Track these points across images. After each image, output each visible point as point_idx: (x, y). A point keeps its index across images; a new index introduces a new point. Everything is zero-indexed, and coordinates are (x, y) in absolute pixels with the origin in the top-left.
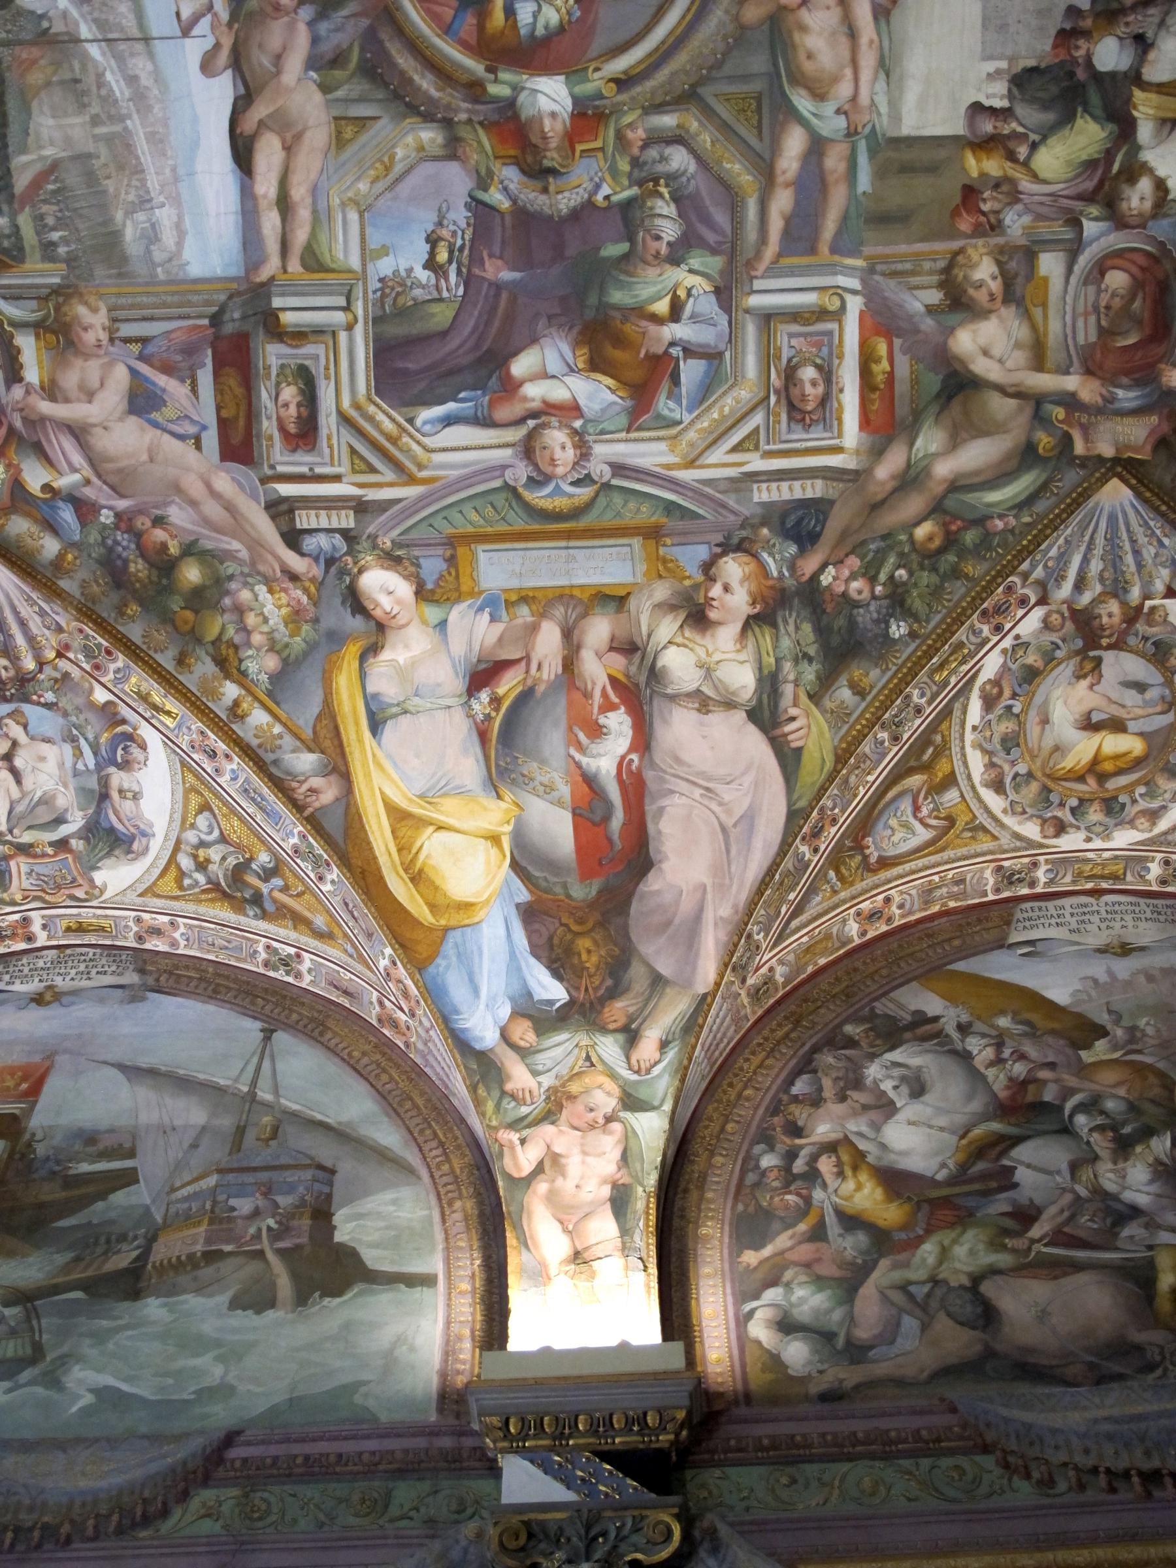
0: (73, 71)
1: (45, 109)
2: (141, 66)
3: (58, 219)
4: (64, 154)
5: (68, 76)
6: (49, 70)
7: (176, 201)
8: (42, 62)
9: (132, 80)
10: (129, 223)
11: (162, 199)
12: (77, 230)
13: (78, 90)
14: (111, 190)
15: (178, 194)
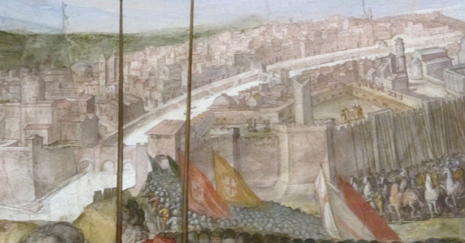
0: (223, 138)
1: (269, 181)
2: (224, 48)
3: (408, 186)
4: (326, 168)
5: (229, 146)
6: (221, 169)
7: (396, 23)
8: (210, 176)
9: (240, 62)
10: (420, 91)
11: (392, 42)
12: (424, 163)
13: (249, 138)
14: (376, 109)
15: (388, 19)
